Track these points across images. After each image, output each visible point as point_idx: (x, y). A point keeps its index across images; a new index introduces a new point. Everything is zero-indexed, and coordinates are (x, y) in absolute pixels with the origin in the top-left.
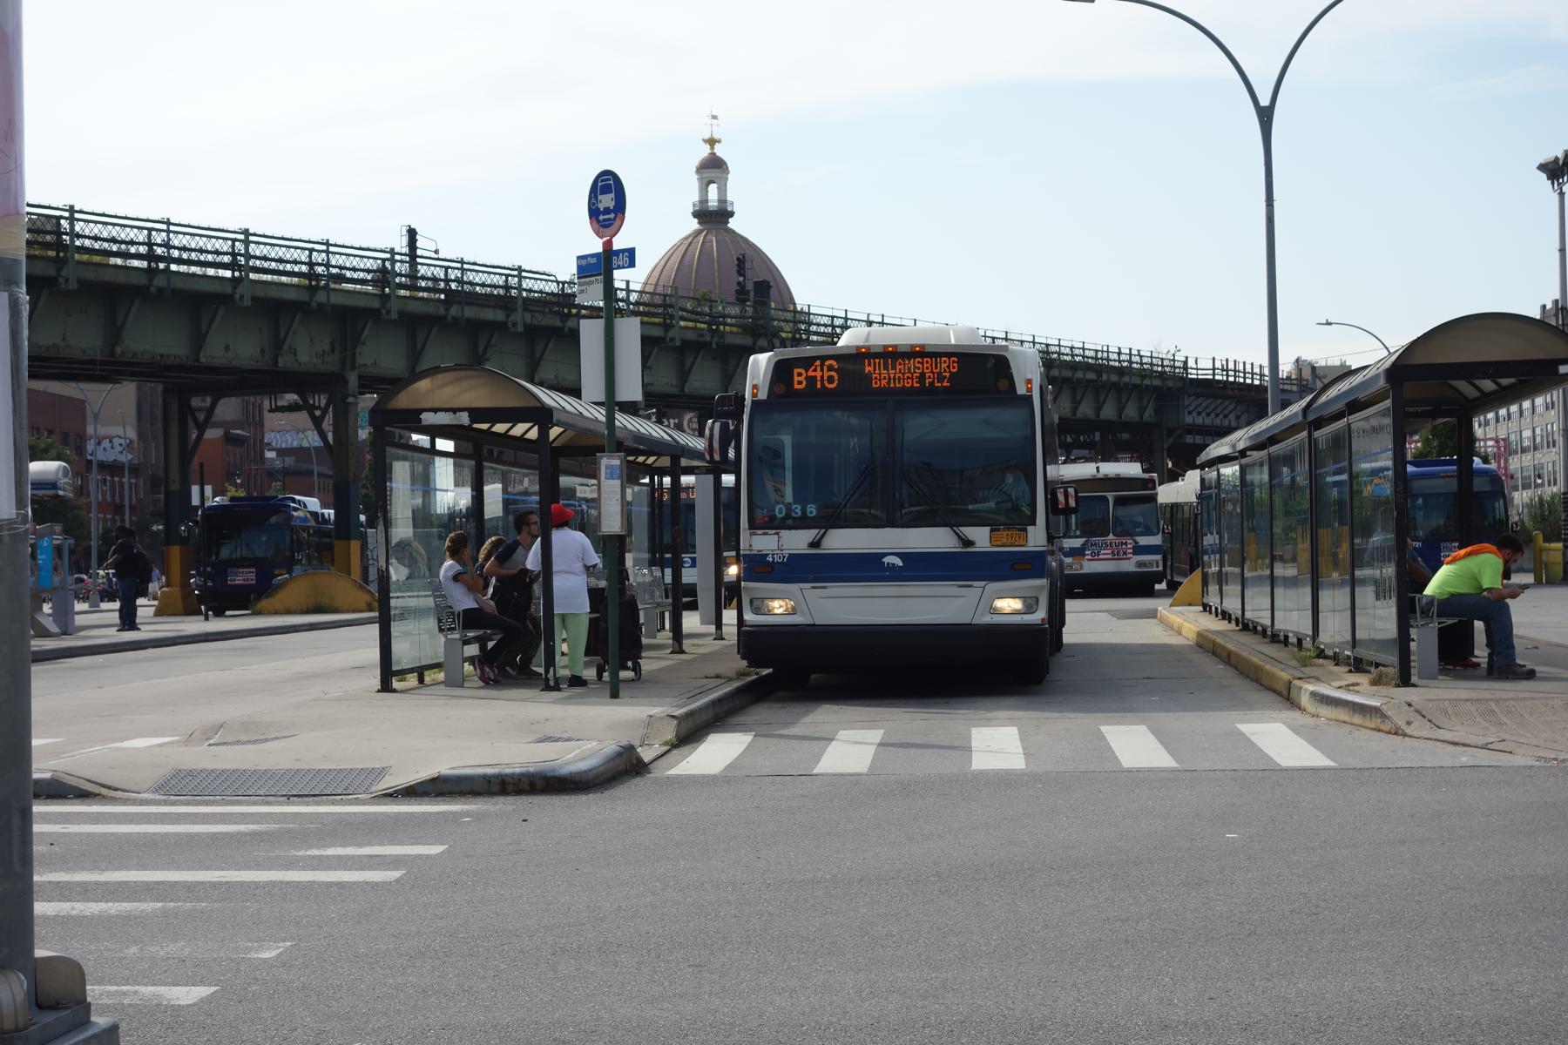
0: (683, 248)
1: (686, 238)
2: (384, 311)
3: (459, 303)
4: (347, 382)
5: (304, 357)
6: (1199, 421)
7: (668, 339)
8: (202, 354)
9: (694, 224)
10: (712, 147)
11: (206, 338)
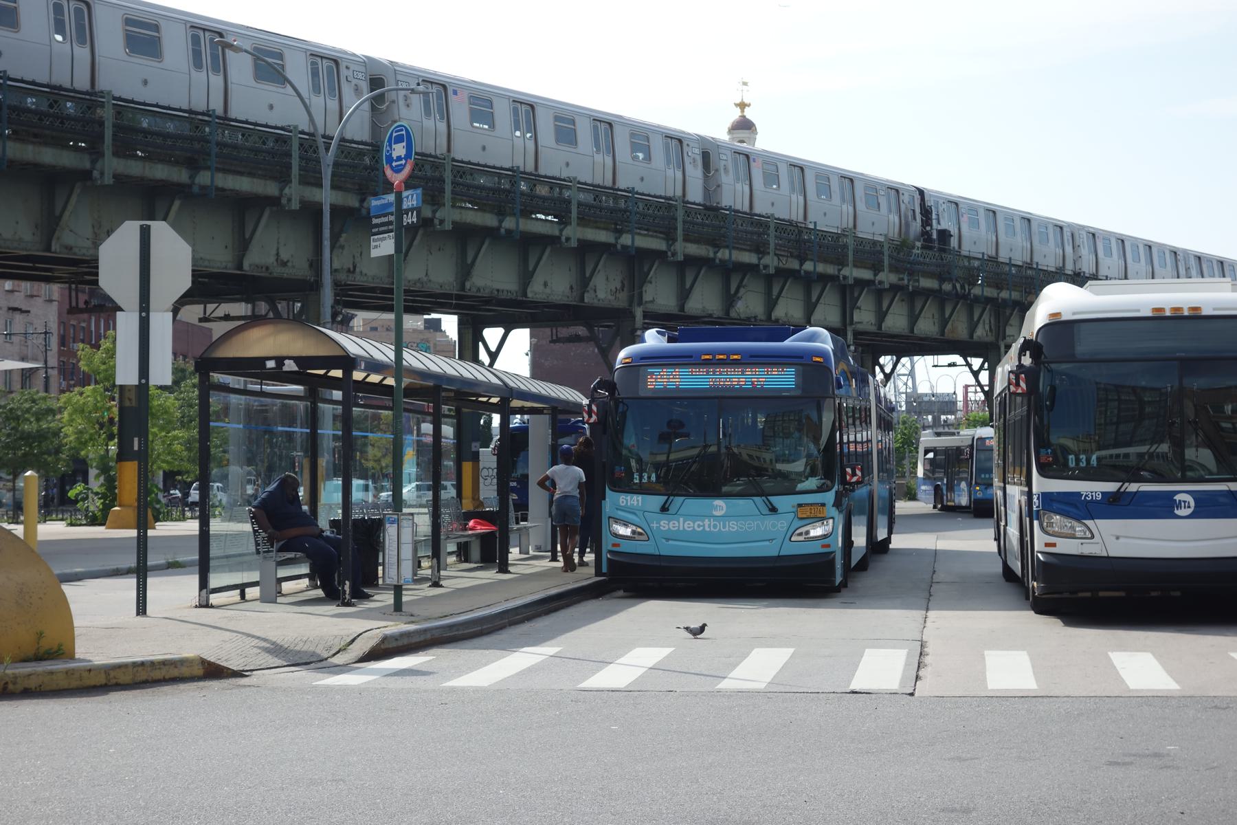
2: (669, 254)
3: (727, 247)
4: (634, 317)
5: (601, 295)
7: (877, 281)
8: (529, 290)
10: (743, 111)
11: (532, 277)
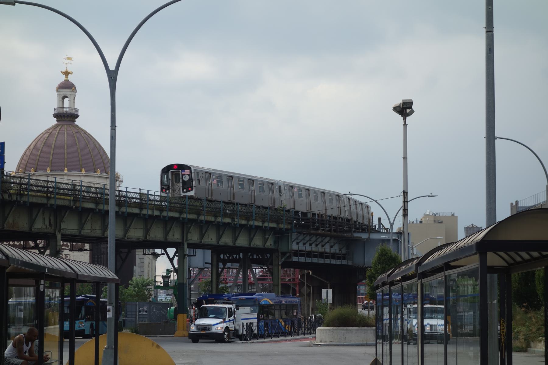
0: (47, 135)
1: (49, 129)
6: (301, 247)
9: (54, 121)
